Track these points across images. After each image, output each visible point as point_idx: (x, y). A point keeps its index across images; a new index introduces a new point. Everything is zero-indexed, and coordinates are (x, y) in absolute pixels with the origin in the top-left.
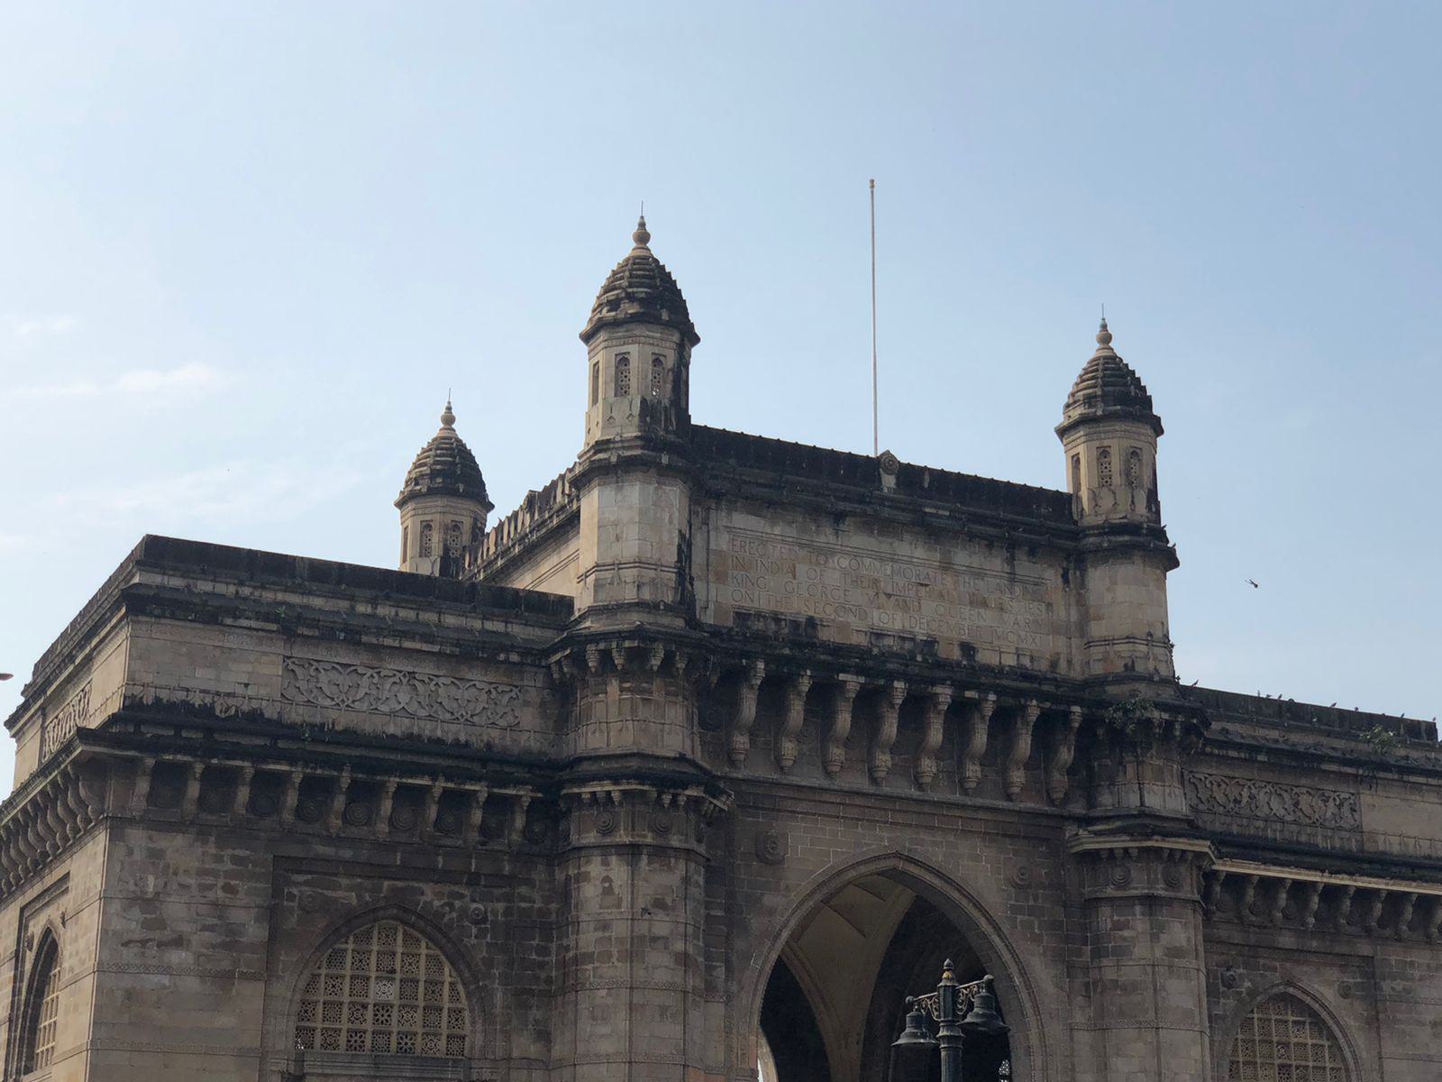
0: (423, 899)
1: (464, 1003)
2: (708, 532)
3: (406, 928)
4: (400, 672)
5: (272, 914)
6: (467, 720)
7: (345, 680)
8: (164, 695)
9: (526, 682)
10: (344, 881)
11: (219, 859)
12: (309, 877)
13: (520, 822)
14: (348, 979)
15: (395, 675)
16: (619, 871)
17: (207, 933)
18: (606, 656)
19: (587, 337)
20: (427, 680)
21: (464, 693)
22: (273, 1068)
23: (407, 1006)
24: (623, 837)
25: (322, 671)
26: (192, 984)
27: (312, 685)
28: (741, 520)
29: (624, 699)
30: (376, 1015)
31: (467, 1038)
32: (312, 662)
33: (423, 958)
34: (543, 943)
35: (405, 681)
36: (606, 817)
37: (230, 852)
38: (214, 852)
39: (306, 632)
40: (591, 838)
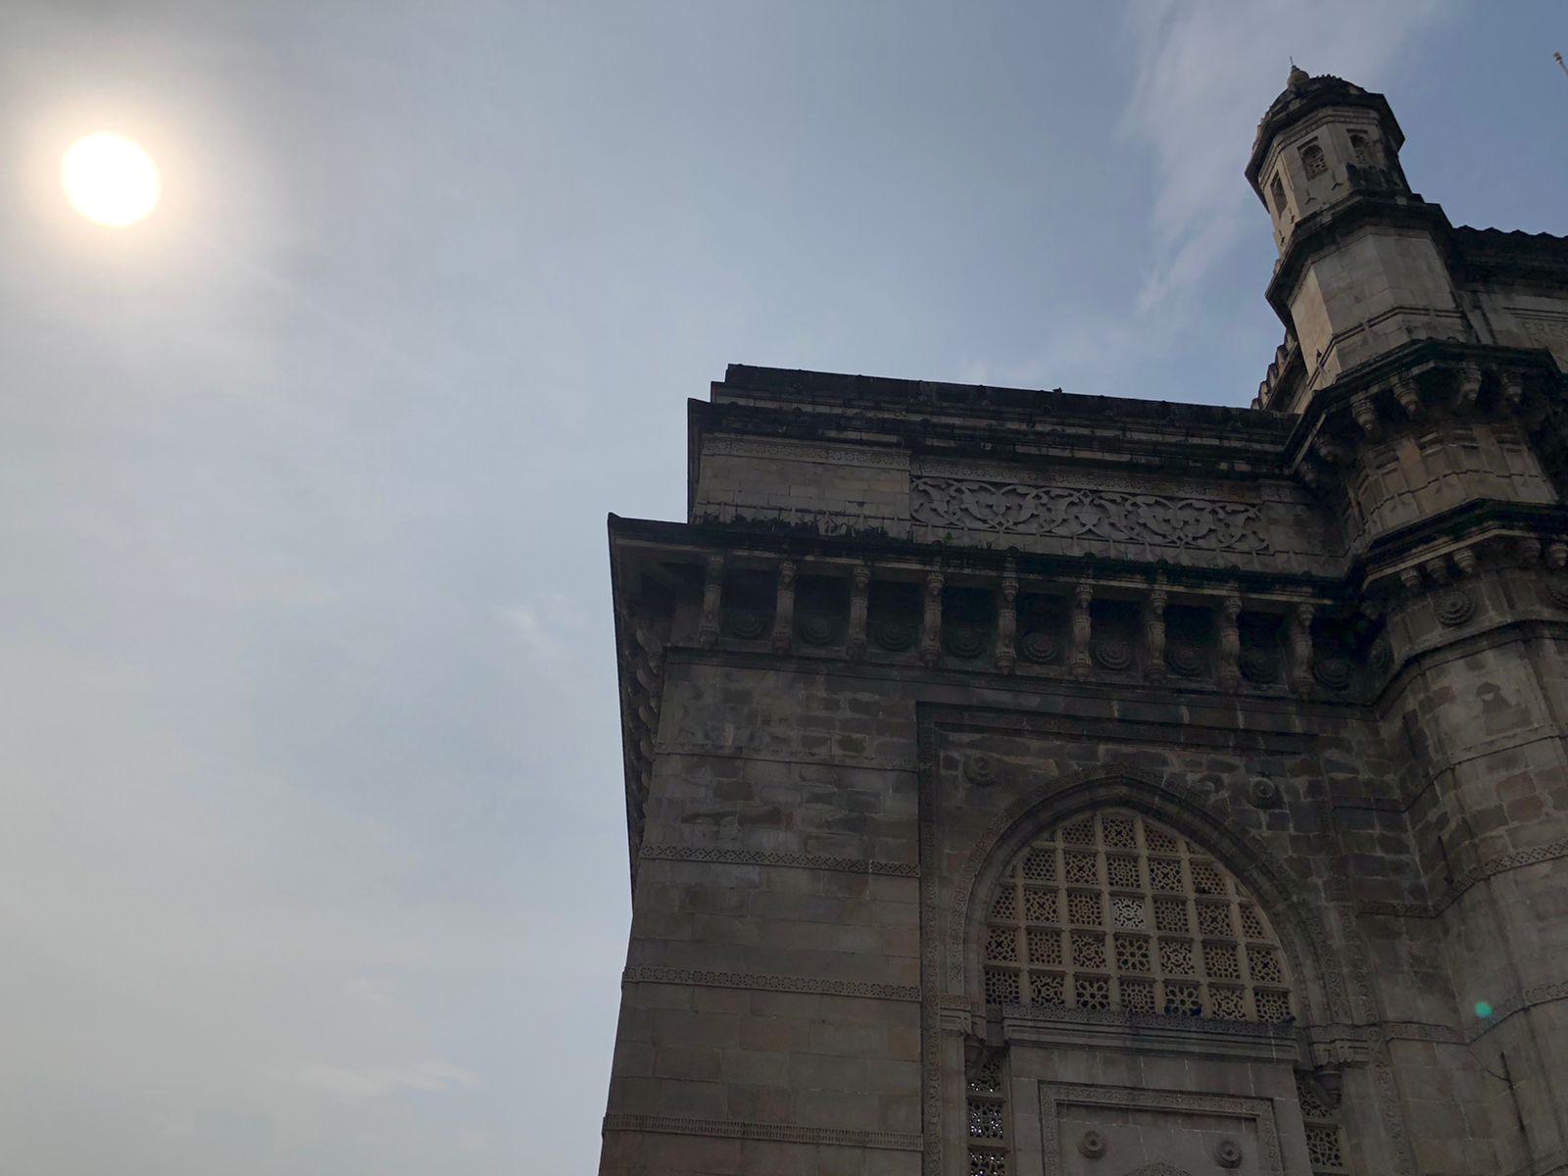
0: (1168, 771)
1: (1271, 936)
2: (1484, 315)
3: (1150, 821)
4: (1079, 490)
5: (923, 781)
6: (1187, 543)
7: (999, 500)
8: (749, 514)
9: (1265, 498)
10: (1035, 744)
11: (832, 705)
12: (977, 736)
13: (1303, 647)
14: (1063, 896)
15: (1071, 495)
16: (1506, 671)
17: (819, 806)
18: (1386, 406)
19: (1254, 172)
20: (1119, 500)
21: (1174, 512)
22: (949, 1026)
23: (1174, 940)
24: (1493, 617)
25: (968, 492)
26: (798, 880)
27: (955, 506)
28: (1526, 301)
29: (1429, 455)
30: (1121, 954)
31: (1292, 999)
32: (951, 482)
33: (1185, 865)
34: (1390, 834)
35: (1087, 501)
36: (1451, 599)
37: (850, 695)
38: (825, 695)
39: (936, 443)
40: (1435, 636)
